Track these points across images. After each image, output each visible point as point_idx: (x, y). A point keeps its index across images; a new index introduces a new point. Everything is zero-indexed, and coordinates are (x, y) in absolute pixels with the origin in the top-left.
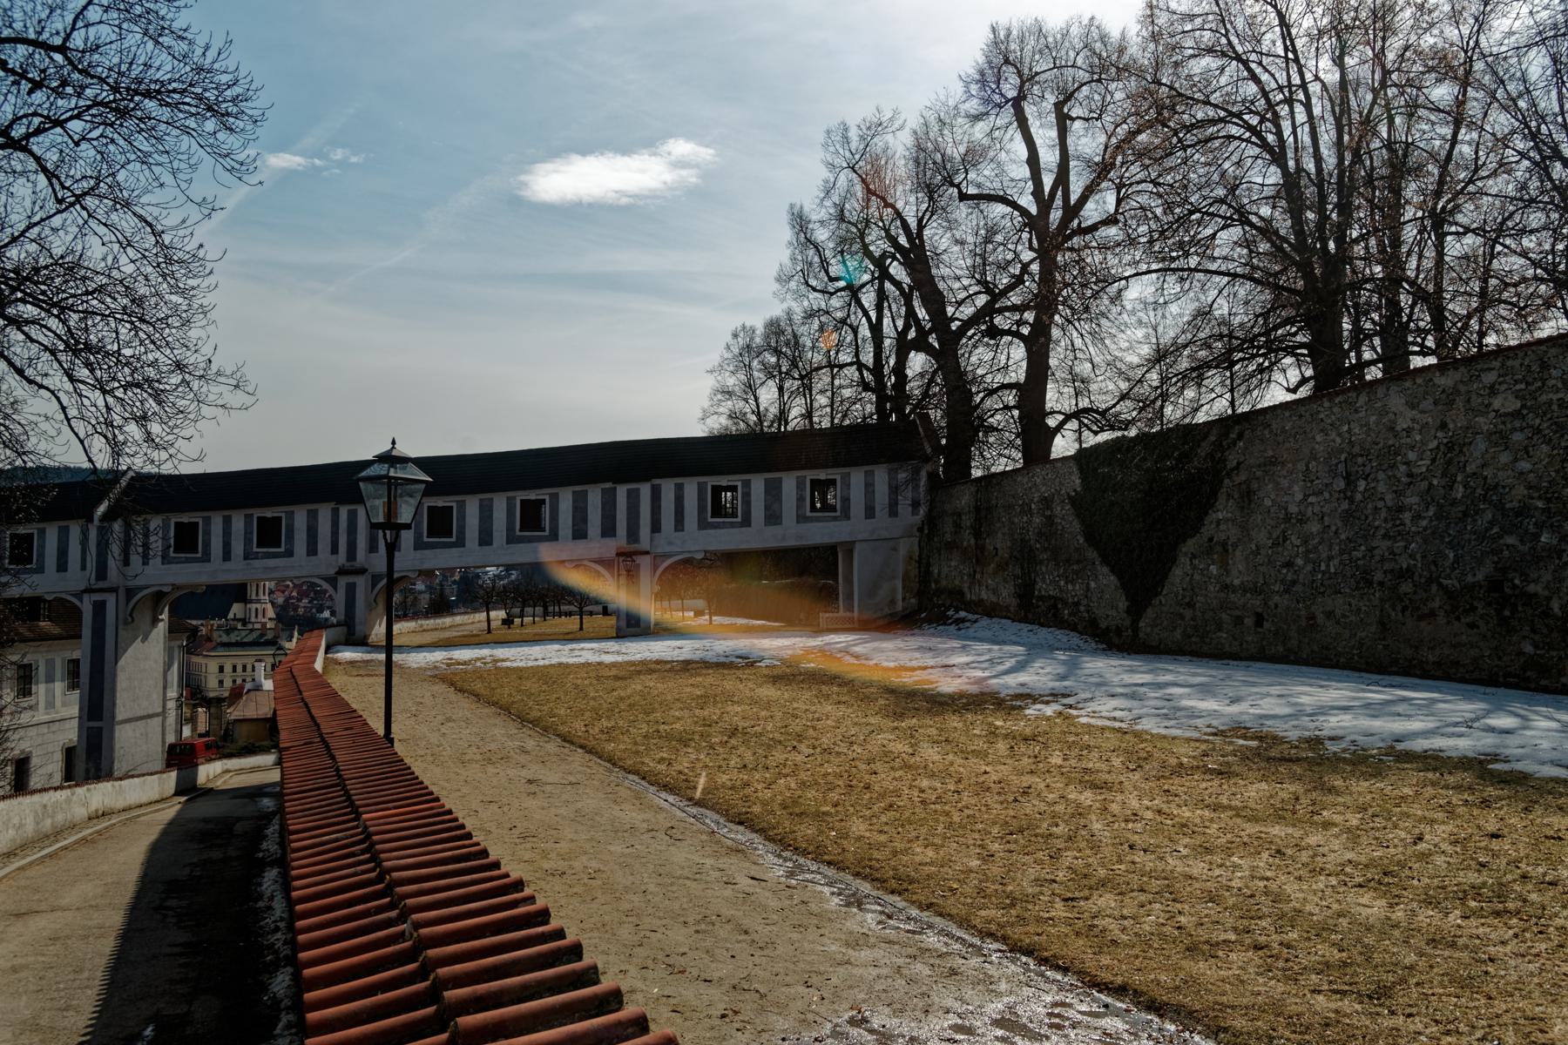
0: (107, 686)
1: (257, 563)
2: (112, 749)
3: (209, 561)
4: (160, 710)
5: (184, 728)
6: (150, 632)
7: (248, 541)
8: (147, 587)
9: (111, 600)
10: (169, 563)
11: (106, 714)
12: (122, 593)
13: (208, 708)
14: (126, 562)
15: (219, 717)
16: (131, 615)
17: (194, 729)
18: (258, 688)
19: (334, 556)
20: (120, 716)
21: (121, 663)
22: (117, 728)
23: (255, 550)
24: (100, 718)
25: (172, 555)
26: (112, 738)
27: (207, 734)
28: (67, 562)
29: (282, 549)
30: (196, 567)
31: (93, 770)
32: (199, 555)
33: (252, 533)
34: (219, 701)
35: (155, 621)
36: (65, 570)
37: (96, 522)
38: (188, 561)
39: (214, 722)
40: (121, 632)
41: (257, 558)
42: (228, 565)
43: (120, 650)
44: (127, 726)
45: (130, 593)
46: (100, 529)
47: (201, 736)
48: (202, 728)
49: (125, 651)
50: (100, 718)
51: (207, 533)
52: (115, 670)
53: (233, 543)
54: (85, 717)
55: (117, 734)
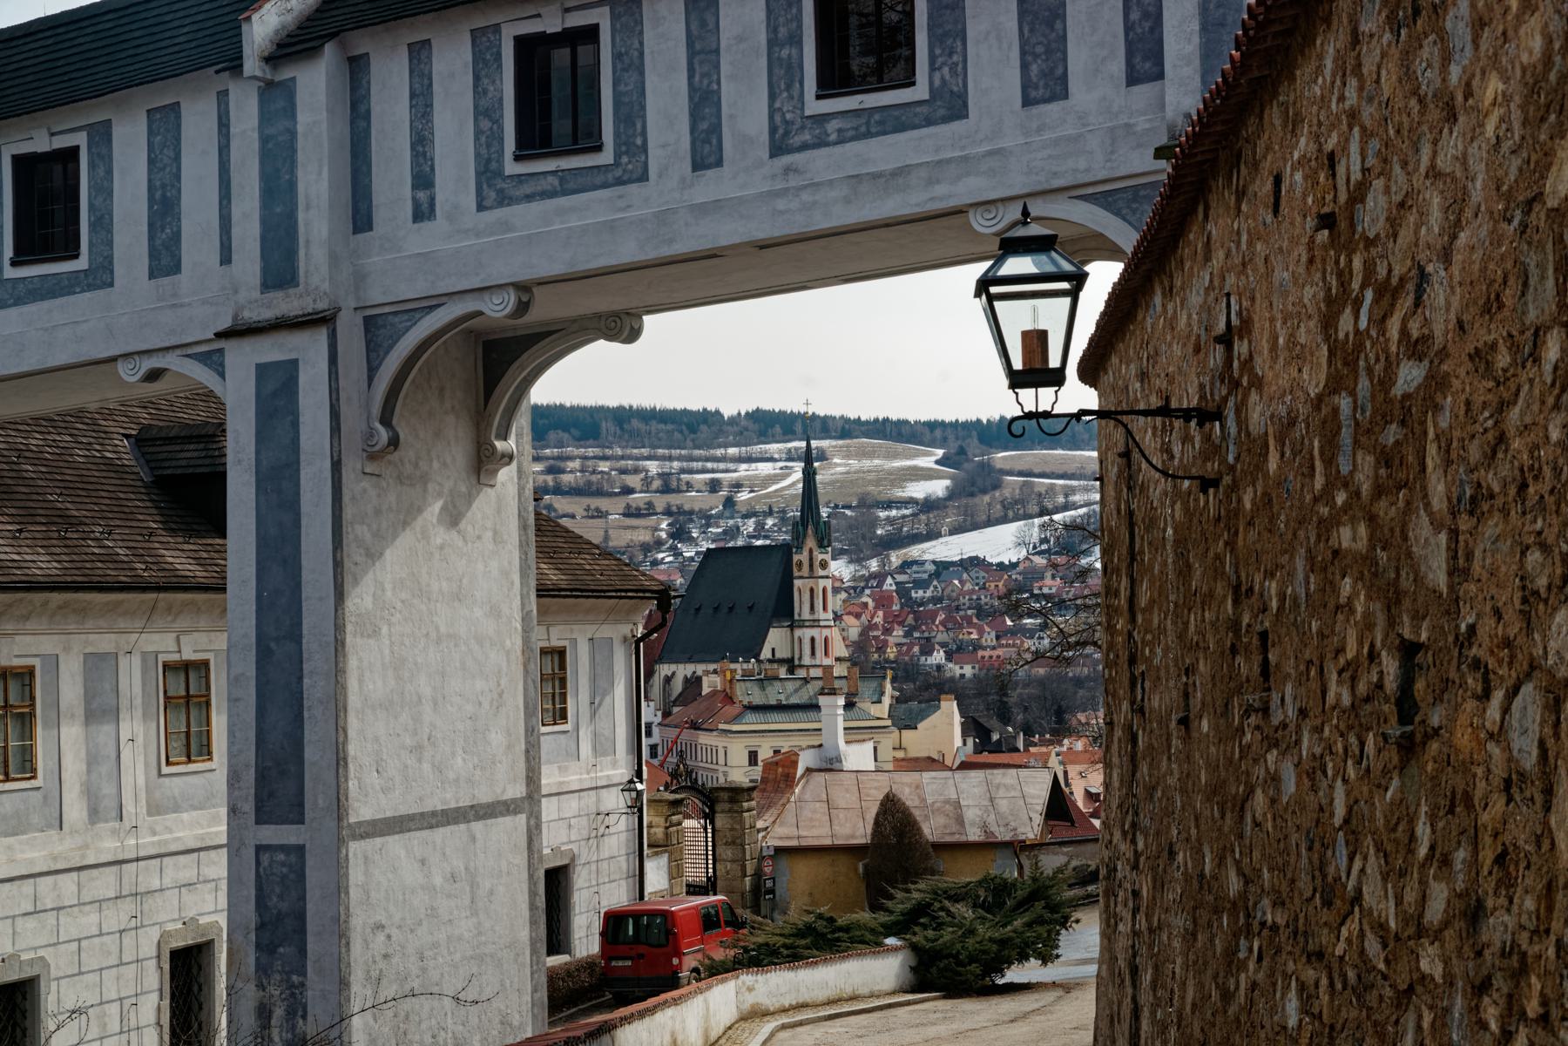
0: (314, 687)
1: (819, 163)
2: (341, 934)
3: (643, 177)
4: (518, 790)
5: (649, 866)
6: (470, 499)
7: (782, 76)
8: (432, 303)
9: (310, 350)
10: (504, 200)
11: (316, 798)
12: (350, 329)
13: (709, 817)
14: (361, 219)
15: (737, 842)
16: (386, 420)
17: (675, 872)
18: (831, 766)
19: (1144, 91)
20: (362, 810)
21: (360, 600)
22: (355, 848)
23: (814, 107)
24: (296, 815)
25: (511, 168)
26: (339, 888)
27: (709, 887)
28: (177, 237)
29: (920, 91)
30: (592, 208)
31: (279, 1013)
32: (606, 157)
33: (796, 40)
34: (736, 794)
35: (484, 462)
36: (176, 268)
37: (251, 65)
38: (568, 185)
39: (726, 853)
40: (353, 484)
41: (821, 143)
42: (711, 186)
43: (353, 553)
44: (394, 844)
45: (378, 331)
46: (268, 88)
47: (693, 890)
48: (696, 871)
49: (373, 556)
50: (296, 815)
51: (631, 64)
52: (339, 628)
53: (727, 90)
54: (249, 807)
55: (356, 875)
